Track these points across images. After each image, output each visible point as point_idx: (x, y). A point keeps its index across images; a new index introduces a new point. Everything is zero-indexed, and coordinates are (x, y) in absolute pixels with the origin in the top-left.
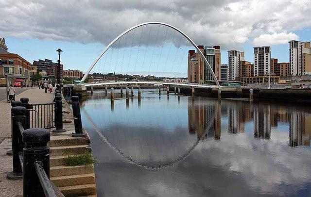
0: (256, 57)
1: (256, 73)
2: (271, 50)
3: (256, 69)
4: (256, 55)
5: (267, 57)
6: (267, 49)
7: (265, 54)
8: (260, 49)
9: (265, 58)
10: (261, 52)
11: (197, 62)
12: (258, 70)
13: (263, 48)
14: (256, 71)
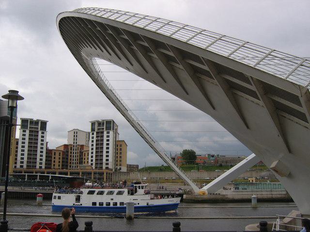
0: (24, 135)
1: (22, 162)
2: (49, 127)
3: (23, 155)
4: (24, 131)
5: (43, 137)
6: (44, 124)
7: (40, 133)
8: (32, 122)
9: (40, 138)
10: (36, 127)
12: (26, 157)
13: (37, 122)
14: (22, 159)
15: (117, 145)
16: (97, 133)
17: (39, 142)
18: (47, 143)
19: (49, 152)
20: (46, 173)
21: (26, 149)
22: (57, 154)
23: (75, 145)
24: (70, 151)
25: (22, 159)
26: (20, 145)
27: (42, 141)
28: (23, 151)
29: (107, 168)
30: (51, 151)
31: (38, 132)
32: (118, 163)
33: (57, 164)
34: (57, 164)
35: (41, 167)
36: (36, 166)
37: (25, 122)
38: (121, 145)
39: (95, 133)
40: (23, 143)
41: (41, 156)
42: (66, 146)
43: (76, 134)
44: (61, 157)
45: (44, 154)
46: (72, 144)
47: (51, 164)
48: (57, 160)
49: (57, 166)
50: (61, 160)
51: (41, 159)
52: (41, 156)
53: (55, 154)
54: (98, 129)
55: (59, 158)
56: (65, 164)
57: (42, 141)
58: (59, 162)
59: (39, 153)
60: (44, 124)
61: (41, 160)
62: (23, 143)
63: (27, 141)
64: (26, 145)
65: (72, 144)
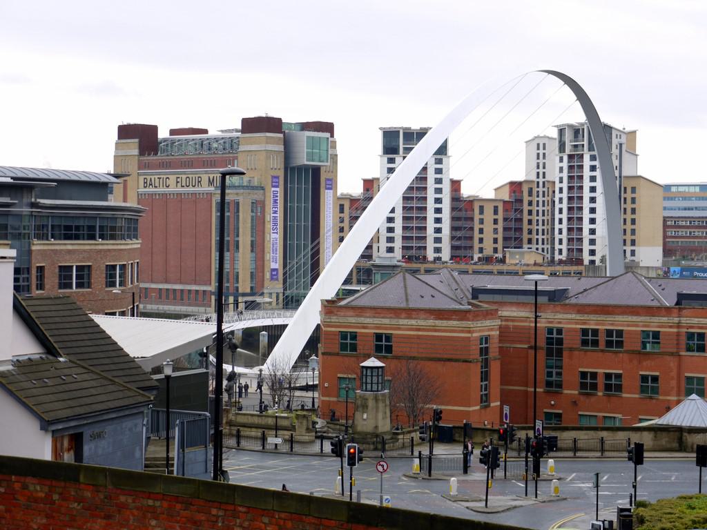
5: (439, 171)
11: (257, 196)
15: (625, 188)
16: (571, 157)
18: (456, 185)
19: (463, 208)
22: (489, 210)
23: (541, 180)
24: (526, 199)
27: (439, 181)
30: (470, 202)
32: (629, 237)
33: (488, 236)
34: (488, 236)
38: (634, 190)
39: (565, 159)
42: (515, 186)
43: (541, 152)
44: (500, 217)
45: (446, 215)
46: (533, 177)
47: (471, 238)
48: (488, 227)
50: (500, 226)
53: (481, 212)
54: (576, 146)
55: (496, 222)
56: (514, 235)
57: (439, 181)
58: (496, 231)
65: (533, 177)
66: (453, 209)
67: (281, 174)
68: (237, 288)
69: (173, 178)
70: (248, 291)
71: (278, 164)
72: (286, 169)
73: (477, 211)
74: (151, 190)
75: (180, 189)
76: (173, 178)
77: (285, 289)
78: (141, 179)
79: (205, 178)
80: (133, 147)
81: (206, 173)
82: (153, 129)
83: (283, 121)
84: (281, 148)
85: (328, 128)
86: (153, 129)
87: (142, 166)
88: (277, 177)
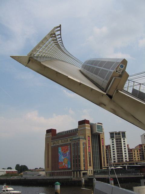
0: (113, 142)
1: (114, 159)
3: (114, 154)
5: (124, 142)
6: (124, 134)
7: (122, 139)
8: (116, 134)
9: (123, 143)
13: (119, 133)
14: (114, 157)
17: (123, 145)
19: (130, 151)
20: (121, 164)
21: (115, 150)
22: (136, 151)
25: (114, 157)
26: (112, 148)
27: (124, 144)
28: (114, 152)
29: (126, 161)
30: (131, 150)
31: (121, 139)
33: (137, 158)
34: (137, 158)
35: (126, 161)
36: (123, 161)
37: (112, 135)
40: (113, 147)
41: (125, 154)
42: (141, 145)
45: (127, 152)
48: (136, 155)
49: (137, 159)
51: (126, 156)
52: (125, 154)
57: (124, 144)
59: (124, 152)
60: (124, 134)
61: (126, 156)
62: (113, 147)
63: (115, 145)
64: (115, 148)
66: (128, 151)
67: (90, 135)
68: (80, 169)
69: (60, 141)
70: (83, 169)
71: (88, 133)
72: (91, 134)
73: (133, 151)
74: (55, 145)
75: (62, 144)
76: (60, 141)
77: (93, 169)
78: (52, 142)
79: (69, 139)
80: (50, 135)
81: (69, 138)
82: (55, 130)
83: (90, 122)
84: (90, 128)
85: (102, 124)
86: (55, 130)
87: (52, 139)
88: (89, 136)
